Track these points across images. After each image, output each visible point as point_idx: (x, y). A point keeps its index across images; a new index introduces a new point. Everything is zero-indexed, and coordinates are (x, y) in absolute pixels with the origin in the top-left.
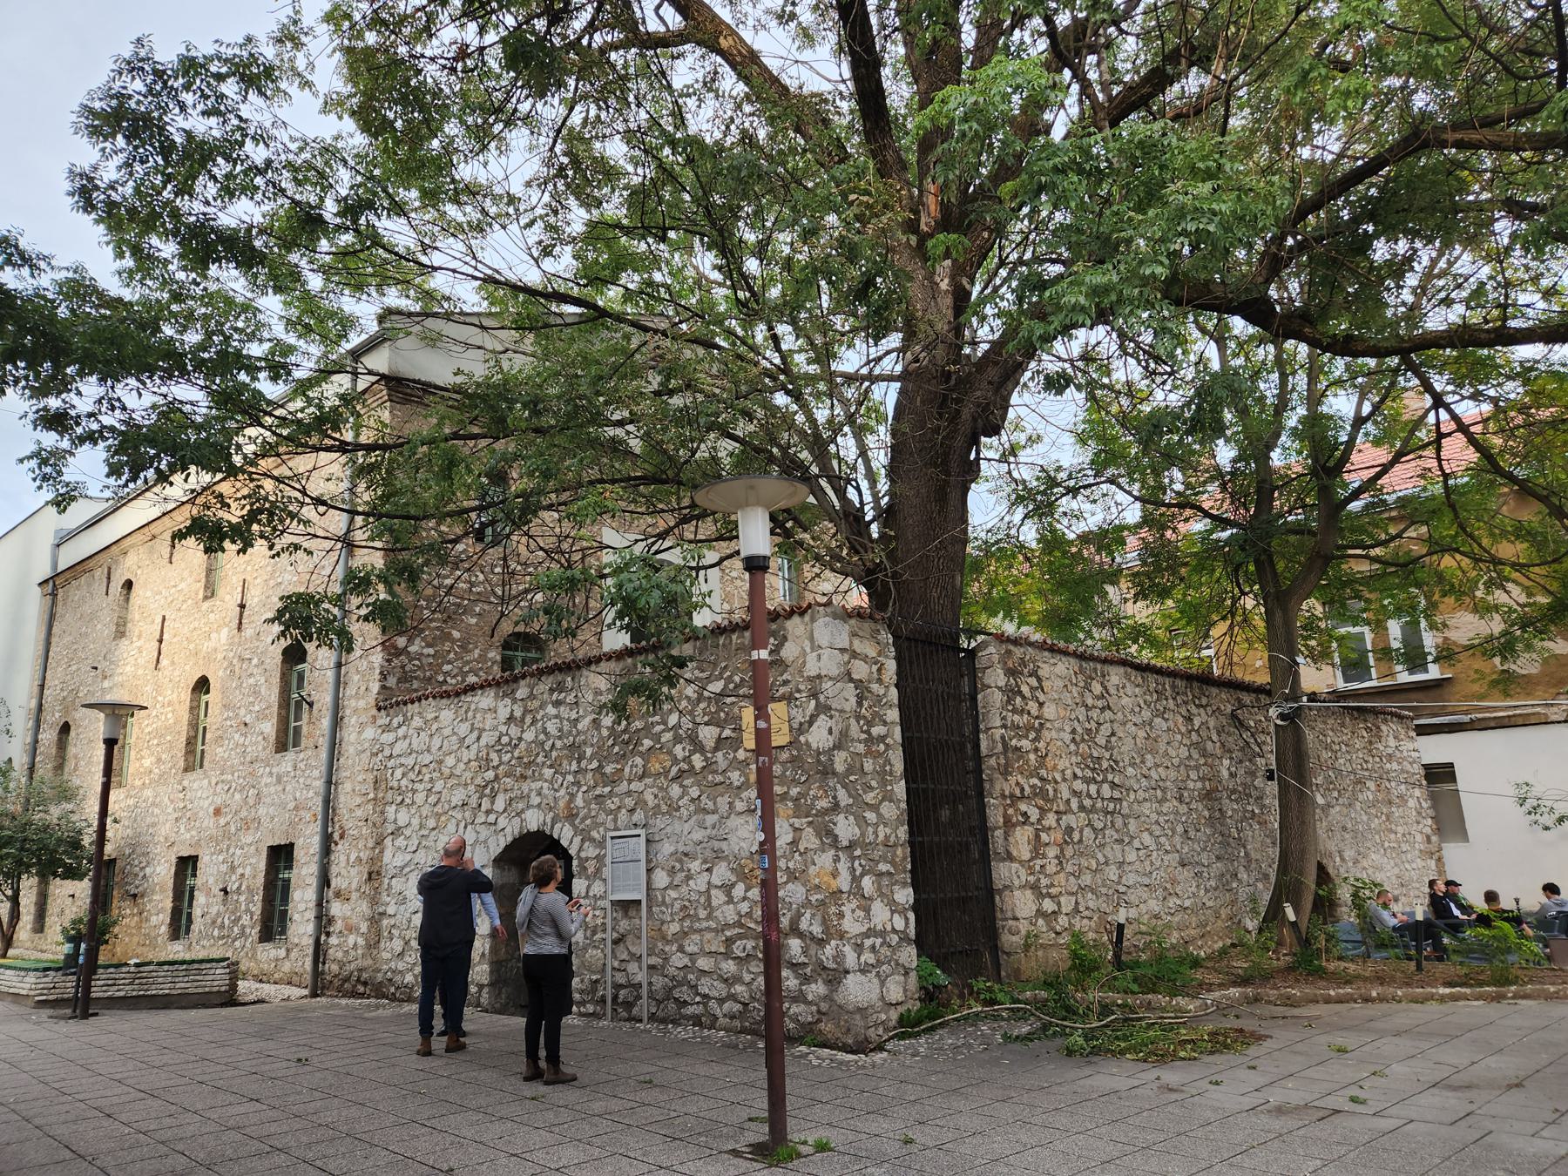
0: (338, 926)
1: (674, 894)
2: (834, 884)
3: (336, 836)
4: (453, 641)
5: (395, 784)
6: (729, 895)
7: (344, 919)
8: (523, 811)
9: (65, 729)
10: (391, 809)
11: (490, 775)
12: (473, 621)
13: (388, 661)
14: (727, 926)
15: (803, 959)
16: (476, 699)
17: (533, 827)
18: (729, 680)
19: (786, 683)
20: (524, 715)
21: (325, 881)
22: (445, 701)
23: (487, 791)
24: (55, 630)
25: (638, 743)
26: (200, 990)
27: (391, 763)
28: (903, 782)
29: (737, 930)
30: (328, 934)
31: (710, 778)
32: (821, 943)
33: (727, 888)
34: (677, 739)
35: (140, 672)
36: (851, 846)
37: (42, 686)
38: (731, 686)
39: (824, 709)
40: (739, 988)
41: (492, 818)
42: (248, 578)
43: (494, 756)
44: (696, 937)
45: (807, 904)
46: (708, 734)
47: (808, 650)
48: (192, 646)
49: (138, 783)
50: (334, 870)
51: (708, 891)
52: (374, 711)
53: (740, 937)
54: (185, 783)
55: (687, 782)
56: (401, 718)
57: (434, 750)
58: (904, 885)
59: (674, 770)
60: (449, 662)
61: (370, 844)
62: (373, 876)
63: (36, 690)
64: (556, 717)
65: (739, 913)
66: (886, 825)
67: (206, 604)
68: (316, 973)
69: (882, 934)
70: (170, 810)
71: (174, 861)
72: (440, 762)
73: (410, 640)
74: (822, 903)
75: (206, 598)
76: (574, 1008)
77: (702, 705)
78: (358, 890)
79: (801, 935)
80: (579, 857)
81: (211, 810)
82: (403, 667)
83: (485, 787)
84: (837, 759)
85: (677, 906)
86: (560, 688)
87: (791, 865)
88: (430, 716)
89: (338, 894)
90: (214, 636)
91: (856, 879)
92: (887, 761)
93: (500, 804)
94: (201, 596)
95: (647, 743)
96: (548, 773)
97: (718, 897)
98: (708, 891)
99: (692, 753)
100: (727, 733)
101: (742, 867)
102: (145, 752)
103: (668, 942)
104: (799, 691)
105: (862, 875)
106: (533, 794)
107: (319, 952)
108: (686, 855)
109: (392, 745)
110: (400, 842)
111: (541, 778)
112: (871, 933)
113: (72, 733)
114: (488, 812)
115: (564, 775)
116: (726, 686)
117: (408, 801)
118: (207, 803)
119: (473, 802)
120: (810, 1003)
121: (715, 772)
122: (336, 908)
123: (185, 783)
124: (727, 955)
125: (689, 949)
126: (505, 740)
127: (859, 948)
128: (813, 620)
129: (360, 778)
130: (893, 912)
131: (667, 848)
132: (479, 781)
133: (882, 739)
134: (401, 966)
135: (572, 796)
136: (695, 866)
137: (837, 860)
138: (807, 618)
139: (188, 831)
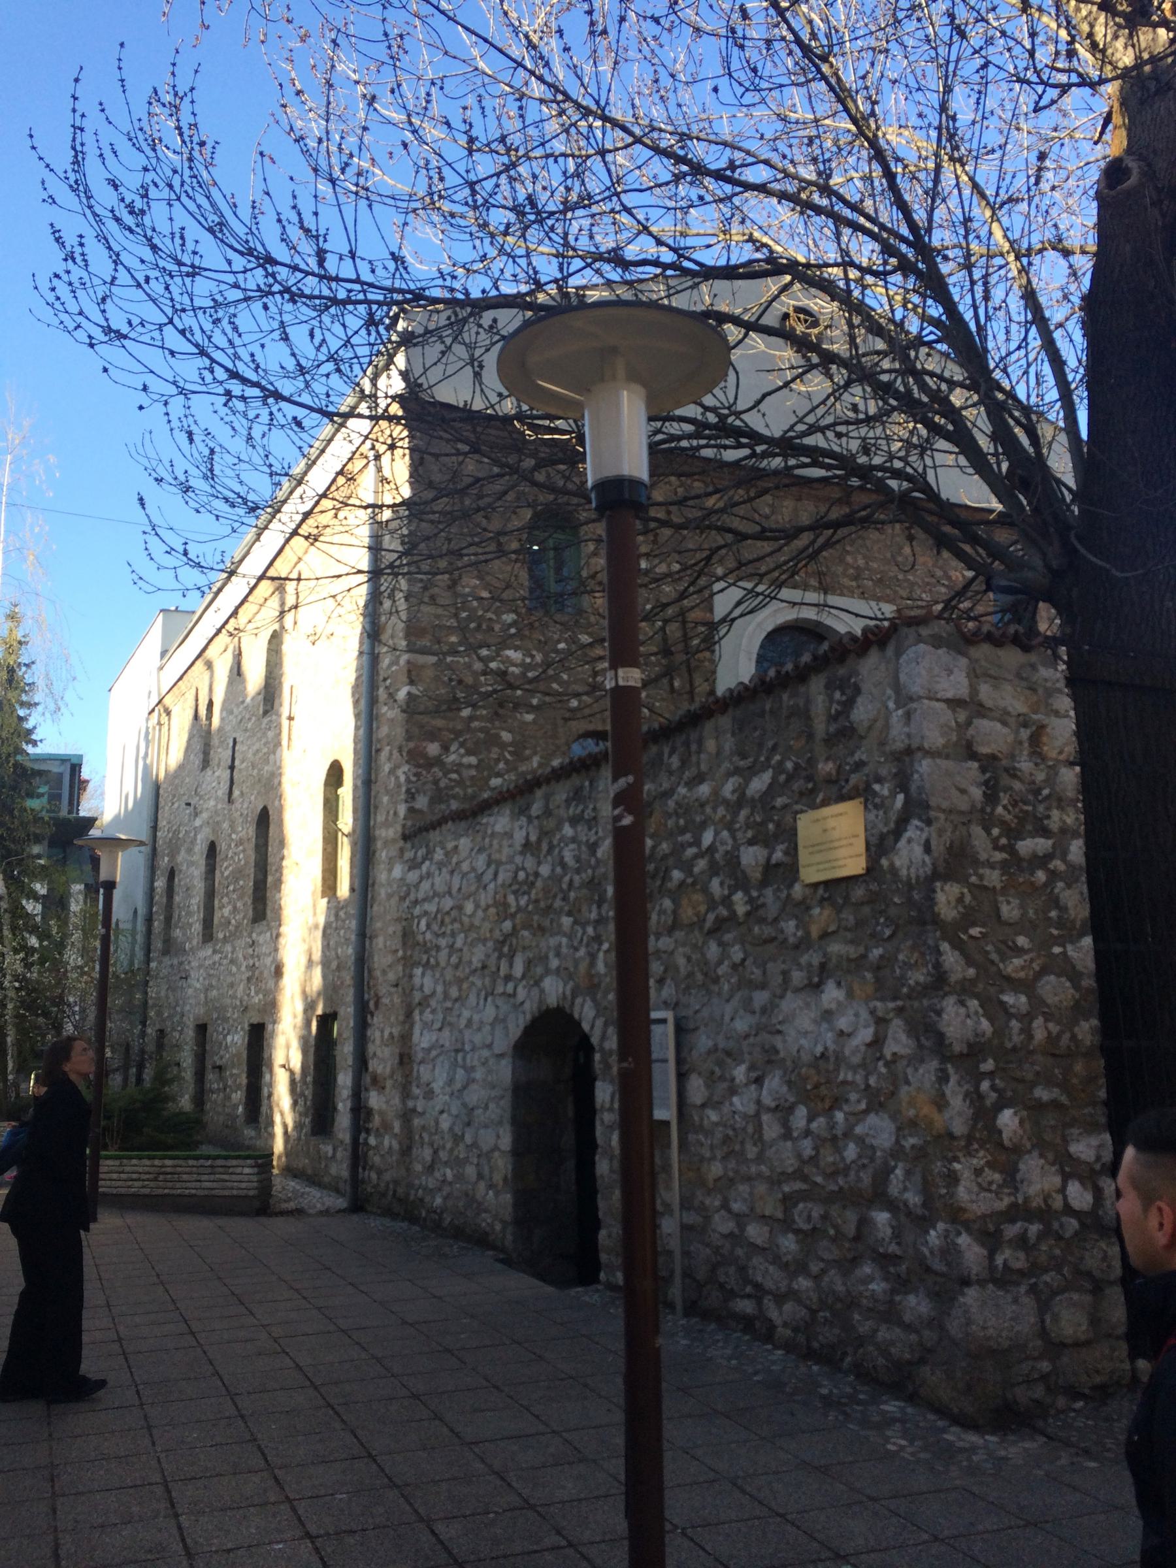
0: (376, 1121)
1: (713, 1116)
2: (939, 1121)
3: (372, 1004)
4: (503, 746)
5: (420, 938)
6: (786, 1125)
7: (381, 1113)
8: (541, 978)
9: (172, 875)
10: (418, 971)
11: (507, 925)
12: (529, 717)
13: (415, 775)
14: (786, 1177)
15: (893, 1248)
16: (492, 819)
17: (552, 1001)
18: (779, 768)
19: (859, 765)
20: (539, 841)
21: (362, 1061)
22: (463, 824)
23: (506, 949)
25: (666, 877)
26: (226, 1193)
27: (417, 911)
28: (1087, 941)
29: (799, 1185)
30: (368, 1131)
31: (756, 929)
32: (924, 1222)
33: (783, 1111)
34: (714, 869)
36: (975, 1050)
38: (782, 778)
39: (916, 808)
40: (803, 1283)
41: (510, 987)
43: (511, 899)
44: (743, 1188)
45: (897, 1152)
46: (751, 857)
47: (891, 705)
49: (221, 936)
50: (371, 1049)
51: (757, 1115)
52: (401, 843)
53: (804, 1196)
55: (728, 937)
56: (421, 852)
57: (454, 890)
58: (1091, 1128)
59: (711, 917)
60: (498, 775)
61: (401, 1018)
62: (405, 1059)
64: (574, 840)
65: (799, 1156)
66: (1048, 1017)
67: (265, 720)
68: (356, 1181)
69: (1044, 1214)
70: (243, 969)
71: (247, 1027)
72: (460, 908)
73: (446, 748)
74: (920, 1154)
76: (602, 1276)
77: (744, 813)
78: (391, 1076)
79: (891, 1205)
80: (602, 1050)
82: (436, 782)
83: (503, 942)
84: (941, 897)
85: (719, 1135)
86: (577, 796)
87: (872, 1081)
88: (450, 845)
89: (375, 1080)
91: (984, 1116)
92: (1056, 902)
93: (518, 970)
95: (677, 875)
96: (566, 921)
97: (771, 1129)
98: (757, 1115)
99: (733, 890)
100: (778, 855)
101: (805, 1079)
102: (225, 900)
103: (709, 1192)
104: (879, 780)
105: (999, 1107)
106: (551, 955)
107: (358, 1156)
108: (728, 1053)
109: (417, 886)
110: (428, 1016)
111: (560, 932)
112: (1014, 1213)
114: (508, 978)
115: (584, 926)
116: (774, 779)
117: (432, 960)
119: (492, 962)
120: (908, 1328)
121: (762, 921)
122: (374, 1100)
124: (787, 1224)
125: (736, 1206)
126: (522, 875)
127: (991, 1239)
128: (899, 654)
129: (391, 930)
130: (1066, 1178)
131: (703, 1042)
132: (497, 934)
133: (1041, 861)
134: (431, 1183)
135: (593, 957)
136: (740, 1073)
137: (943, 1078)
138: (890, 651)
139: (257, 993)
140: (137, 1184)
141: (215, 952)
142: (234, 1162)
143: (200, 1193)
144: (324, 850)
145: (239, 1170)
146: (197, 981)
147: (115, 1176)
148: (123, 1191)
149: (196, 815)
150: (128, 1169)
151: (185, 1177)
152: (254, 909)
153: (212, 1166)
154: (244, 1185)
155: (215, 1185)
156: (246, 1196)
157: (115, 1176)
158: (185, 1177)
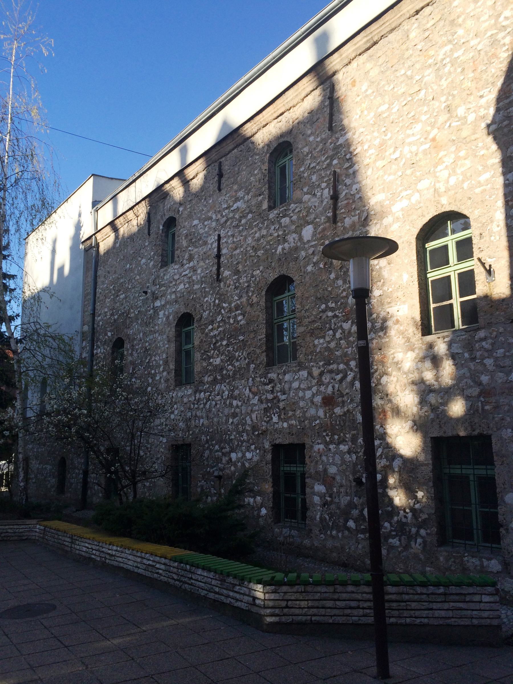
24: (99, 273)
26: (466, 622)
35: (196, 287)
37: (93, 315)
42: (338, 170)
48: (260, 253)
54: (272, 375)
63: (89, 319)
70: (255, 401)
75: (271, 208)
81: (318, 399)
90: (292, 238)
94: (265, 206)
113: (127, 345)
118: (308, 394)
123: (272, 375)
140: (355, 612)
141: (195, 393)
142: (471, 590)
143: (435, 622)
144: (420, 294)
145: (477, 598)
146: (402, 401)
147: (329, 604)
148: (341, 620)
149: (155, 298)
150: (344, 596)
151: (414, 605)
152: (267, 356)
153: (445, 594)
154: (486, 614)
155: (450, 614)
156: (490, 626)
157: (329, 604)
158: (414, 605)
